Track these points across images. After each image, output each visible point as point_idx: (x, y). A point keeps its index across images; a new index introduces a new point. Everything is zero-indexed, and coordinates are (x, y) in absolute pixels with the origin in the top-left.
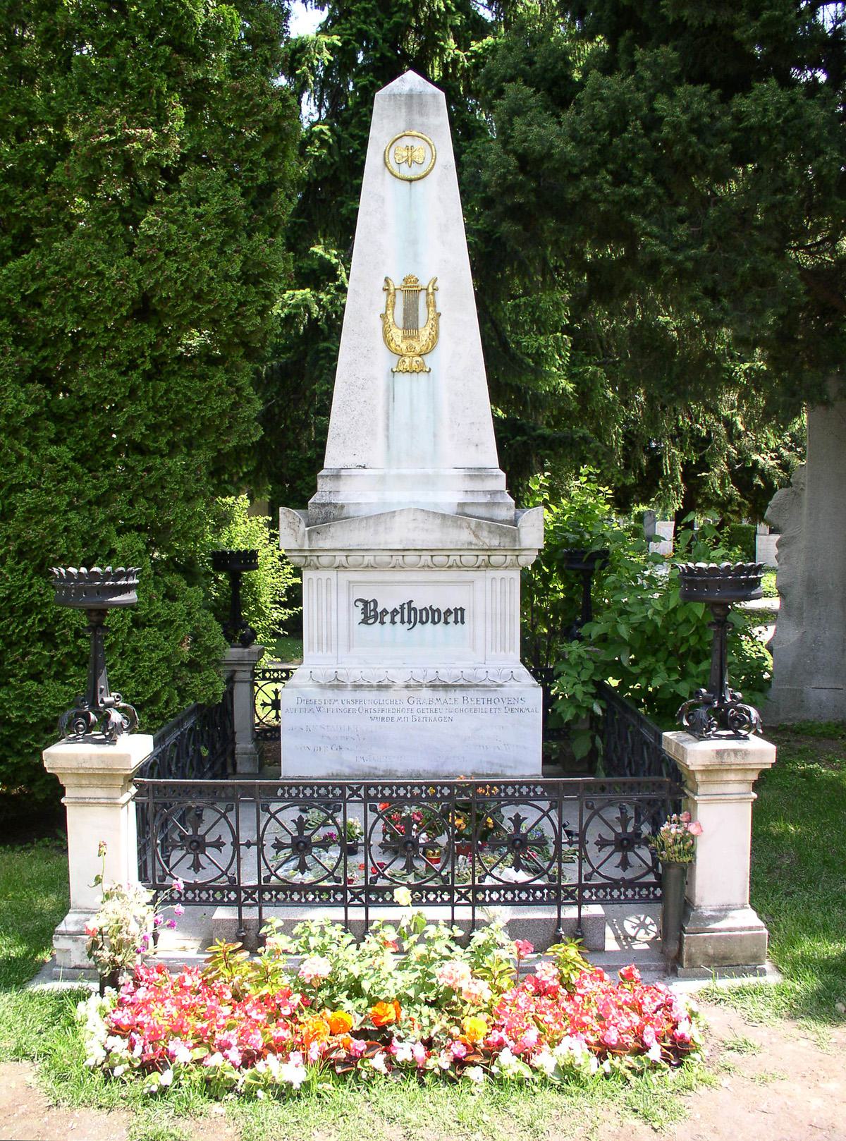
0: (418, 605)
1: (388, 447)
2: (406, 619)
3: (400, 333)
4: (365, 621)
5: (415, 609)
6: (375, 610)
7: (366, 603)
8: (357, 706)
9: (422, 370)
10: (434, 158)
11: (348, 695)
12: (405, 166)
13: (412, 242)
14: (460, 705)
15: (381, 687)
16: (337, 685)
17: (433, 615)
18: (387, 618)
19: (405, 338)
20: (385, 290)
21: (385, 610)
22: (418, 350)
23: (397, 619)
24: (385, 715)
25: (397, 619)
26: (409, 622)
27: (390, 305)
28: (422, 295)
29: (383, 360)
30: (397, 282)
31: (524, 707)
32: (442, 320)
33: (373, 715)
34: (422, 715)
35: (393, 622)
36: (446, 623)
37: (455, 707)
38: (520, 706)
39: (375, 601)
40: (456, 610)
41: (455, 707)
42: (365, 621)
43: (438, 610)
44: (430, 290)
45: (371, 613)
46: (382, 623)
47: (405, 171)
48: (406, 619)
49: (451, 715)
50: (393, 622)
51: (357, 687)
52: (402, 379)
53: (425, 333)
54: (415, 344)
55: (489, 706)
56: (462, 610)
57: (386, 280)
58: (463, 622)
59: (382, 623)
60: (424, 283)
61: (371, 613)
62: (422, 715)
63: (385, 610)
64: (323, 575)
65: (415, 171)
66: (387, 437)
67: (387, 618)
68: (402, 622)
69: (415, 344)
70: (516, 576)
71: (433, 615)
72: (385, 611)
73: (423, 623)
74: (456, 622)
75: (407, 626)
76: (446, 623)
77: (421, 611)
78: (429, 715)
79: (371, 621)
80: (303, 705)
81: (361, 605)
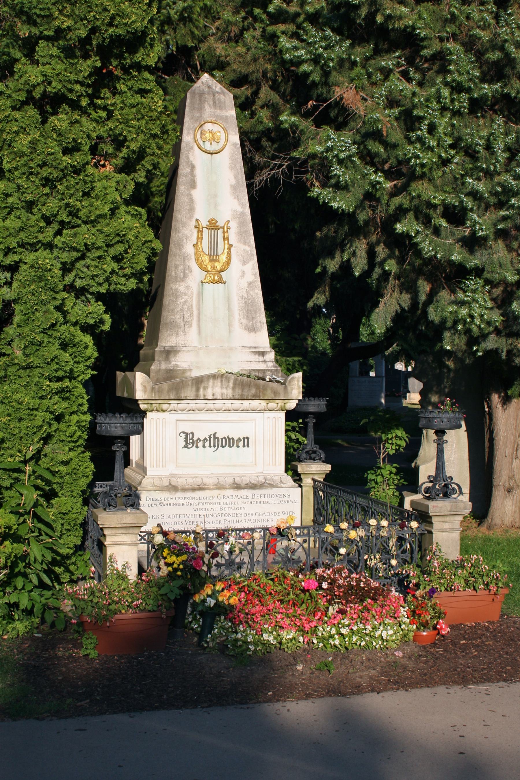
0: (220, 435)
1: (200, 333)
2: (212, 445)
3: (206, 258)
4: (186, 447)
5: (218, 438)
6: (192, 439)
7: (187, 434)
8: (185, 502)
9: (221, 281)
10: (227, 140)
11: (179, 494)
12: (207, 144)
13: (213, 198)
14: (250, 499)
15: (200, 488)
16: (173, 488)
17: (229, 442)
18: (200, 444)
19: (210, 260)
20: (196, 227)
21: (199, 439)
22: (218, 268)
23: (207, 444)
24: (203, 507)
25: (207, 444)
26: (214, 446)
27: (200, 238)
28: (220, 231)
29: (197, 274)
30: (204, 223)
31: (291, 499)
32: (233, 249)
33: (196, 507)
34: (226, 506)
35: (204, 446)
36: (238, 447)
37: (246, 500)
38: (285, 499)
39: (193, 434)
40: (244, 438)
41: (246, 500)
42: (186, 447)
43: (233, 439)
44: (226, 229)
45: (190, 440)
46: (197, 447)
47: (208, 147)
48: (212, 445)
49: (244, 505)
50: (204, 446)
51: (184, 490)
52: (209, 287)
53: (223, 258)
54: (216, 264)
55: (268, 499)
56: (248, 438)
57: (197, 220)
58: (248, 446)
59: (197, 447)
60: (221, 224)
61: (190, 440)
62: (226, 506)
63: (199, 439)
64: (161, 415)
65: (215, 147)
66: (199, 326)
67: (200, 444)
68: (210, 446)
69: (216, 264)
70: (282, 415)
71: (229, 442)
72: (199, 439)
73: (223, 447)
74: (244, 446)
75: (213, 449)
76: (238, 447)
77: (222, 439)
78: (232, 506)
79: (191, 445)
80: (150, 502)
81: (183, 436)
